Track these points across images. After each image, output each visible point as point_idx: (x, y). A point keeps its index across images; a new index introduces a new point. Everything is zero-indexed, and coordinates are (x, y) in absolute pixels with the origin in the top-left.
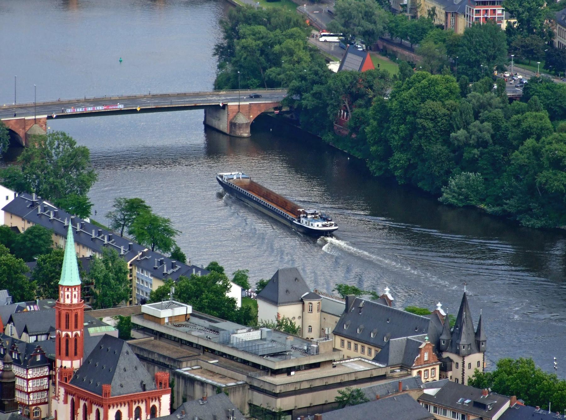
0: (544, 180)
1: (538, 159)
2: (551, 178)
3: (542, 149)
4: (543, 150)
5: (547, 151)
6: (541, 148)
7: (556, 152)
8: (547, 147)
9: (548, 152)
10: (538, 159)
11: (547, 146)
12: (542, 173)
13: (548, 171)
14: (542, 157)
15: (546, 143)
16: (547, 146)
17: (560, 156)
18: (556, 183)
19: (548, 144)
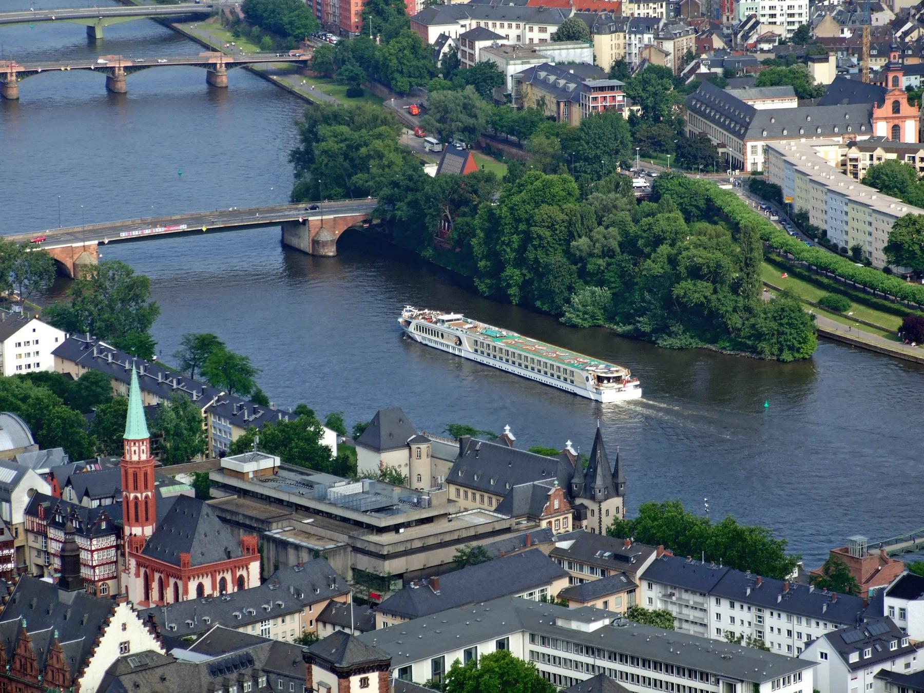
1: (674, 268)
4: (680, 257)
7: (695, 259)
8: (684, 253)
10: (674, 268)
11: (683, 252)
13: (686, 281)
18: (696, 295)
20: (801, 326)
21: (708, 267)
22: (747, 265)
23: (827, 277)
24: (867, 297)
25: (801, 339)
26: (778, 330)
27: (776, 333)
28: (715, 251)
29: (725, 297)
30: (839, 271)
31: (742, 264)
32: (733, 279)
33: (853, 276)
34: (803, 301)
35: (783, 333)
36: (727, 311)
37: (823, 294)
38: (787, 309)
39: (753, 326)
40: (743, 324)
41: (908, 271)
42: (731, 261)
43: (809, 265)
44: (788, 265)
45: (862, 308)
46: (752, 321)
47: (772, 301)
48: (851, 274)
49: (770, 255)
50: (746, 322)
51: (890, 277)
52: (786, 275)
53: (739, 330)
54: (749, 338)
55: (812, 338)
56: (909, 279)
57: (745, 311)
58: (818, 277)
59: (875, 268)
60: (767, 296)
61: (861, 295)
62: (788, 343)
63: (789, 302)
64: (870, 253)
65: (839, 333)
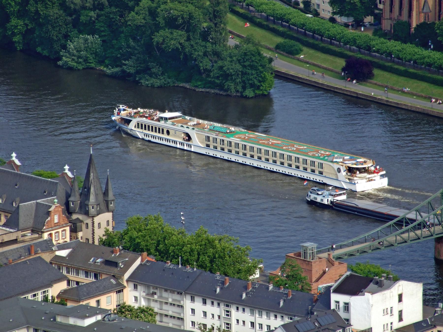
0: (161, 40)
1: (154, 19)
2: (167, 37)
3: (158, 9)
4: (159, 10)
5: (162, 11)
6: (156, 8)
7: (172, 11)
8: (163, 7)
9: (164, 12)
10: (154, 19)
11: (162, 6)
12: (159, 33)
13: (165, 30)
14: (158, 17)
15: (161, 3)
16: (162, 6)
17: (175, 15)
18: (173, 42)
19: (163, 4)
20: (260, 68)
21: (183, 18)
22: (215, 16)
23: (283, 26)
24: (316, 42)
25: (260, 79)
26: (242, 72)
27: (240, 73)
28: (188, 4)
29: (197, 43)
30: (292, 20)
31: (211, 16)
32: (204, 28)
33: (304, 25)
34: (262, 46)
35: (246, 74)
36: (199, 55)
37: (279, 40)
38: (249, 54)
39: (221, 68)
40: (213, 66)
41: (350, 20)
42: (202, 12)
43: (267, 16)
44: (250, 16)
45: (312, 51)
46: (220, 63)
47: (237, 47)
48: (302, 23)
49: (234, 8)
50: (215, 64)
51: (334, 25)
52: (248, 24)
53: (210, 71)
54: (218, 78)
55: (269, 76)
56: (350, 27)
57: (214, 55)
58: (275, 26)
59: (323, 18)
60: (232, 42)
61: (311, 41)
62: (250, 82)
63: (251, 47)
64: (318, 5)
65: (292, 73)
